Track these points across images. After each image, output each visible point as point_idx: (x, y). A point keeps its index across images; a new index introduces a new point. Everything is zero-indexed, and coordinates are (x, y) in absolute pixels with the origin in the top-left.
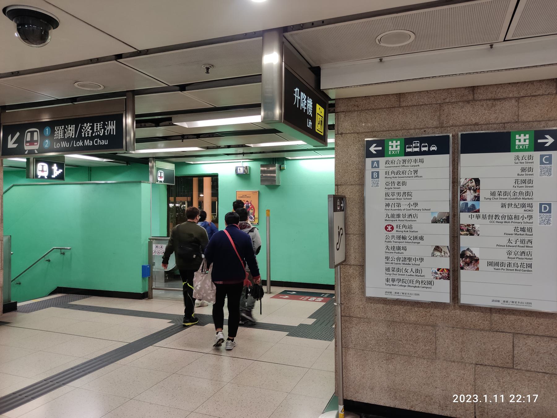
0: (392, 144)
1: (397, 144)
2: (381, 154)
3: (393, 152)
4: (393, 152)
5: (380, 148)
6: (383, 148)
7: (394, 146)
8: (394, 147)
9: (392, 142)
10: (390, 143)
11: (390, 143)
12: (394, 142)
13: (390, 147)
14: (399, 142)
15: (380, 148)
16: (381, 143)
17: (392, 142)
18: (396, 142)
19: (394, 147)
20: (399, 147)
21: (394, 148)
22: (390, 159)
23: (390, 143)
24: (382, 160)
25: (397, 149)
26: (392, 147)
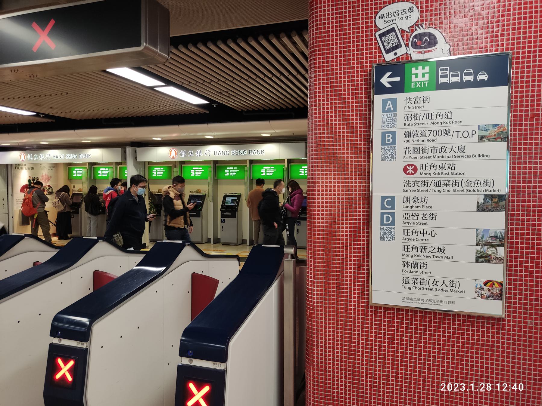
0: (416, 72)
1: (424, 71)
3: (418, 85)
4: (418, 85)
6: (402, 79)
8: (420, 75)
9: (417, 69)
13: (413, 77)
14: (427, 69)
17: (417, 69)
18: (424, 68)
19: (420, 75)
20: (427, 76)
21: (420, 78)
25: (424, 79)
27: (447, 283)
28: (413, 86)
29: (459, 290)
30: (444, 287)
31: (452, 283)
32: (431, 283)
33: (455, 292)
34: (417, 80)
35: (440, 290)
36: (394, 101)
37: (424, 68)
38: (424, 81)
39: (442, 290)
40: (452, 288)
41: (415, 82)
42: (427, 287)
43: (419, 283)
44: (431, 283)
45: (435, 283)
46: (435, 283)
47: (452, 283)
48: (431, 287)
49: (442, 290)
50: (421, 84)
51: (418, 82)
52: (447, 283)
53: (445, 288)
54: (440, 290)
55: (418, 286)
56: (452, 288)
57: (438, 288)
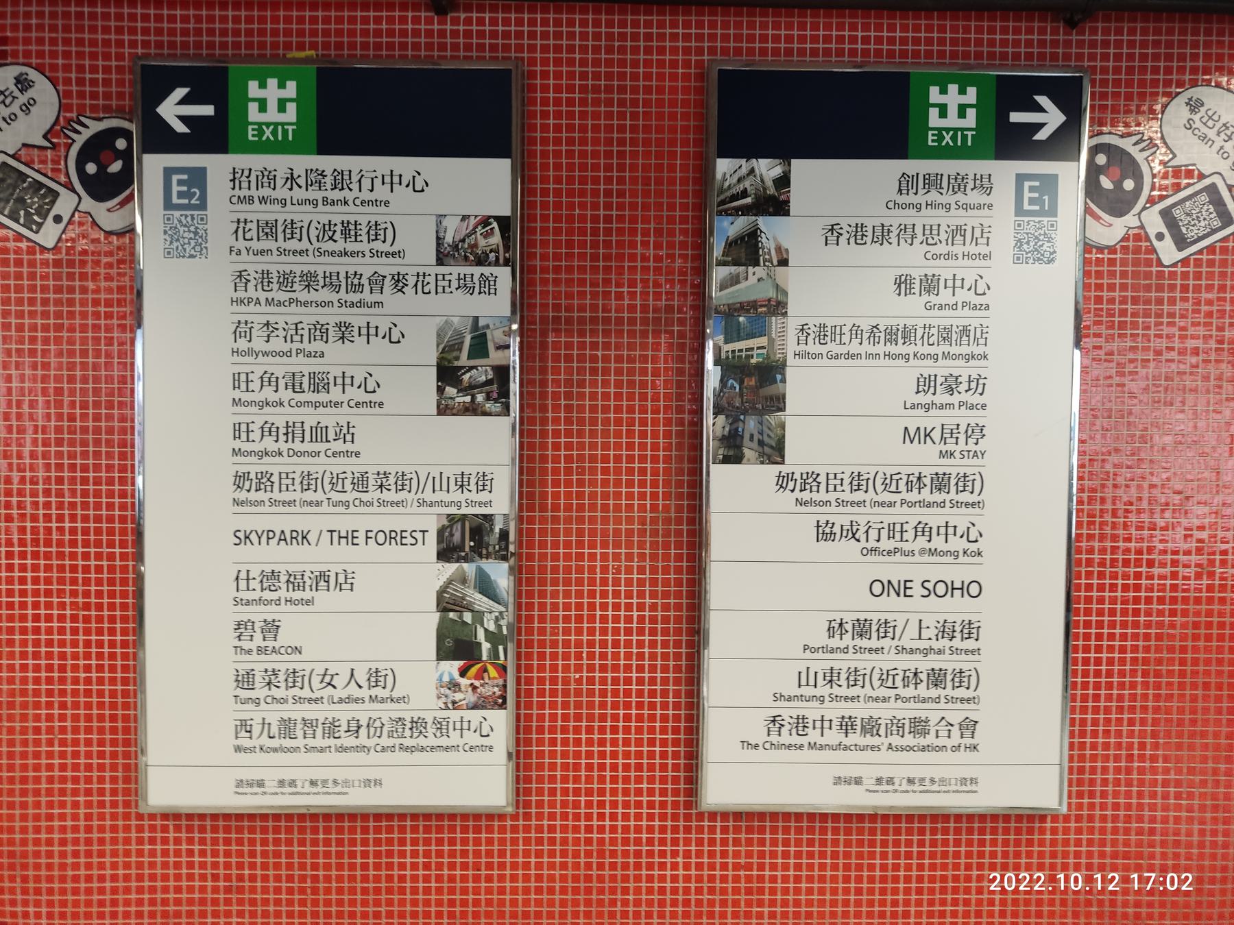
0: (260, 94)
2: (211, 136)
3: (268, 133)
4: (268, 133)
5: (208, 110)
7: (273, 101)
8: (272, 105)
9: (263, 85)
10: (253, 86)
11: (253, 86)
12: (272, 83)
13: (253, 108)
15: (208, 110)
16: (211, 84)
17: (263, 85)
18: (282, 85)
22: (257, 162)
23: (253, 89)
24: (217, 166)
25: (282, 118)
26: (263, 105)
27: (361, 677)
28: (251, 134)
29: (395, 694)
30: (353, 690)
31: (375, 678)
32: (316, 680)
33: (383, 700)
34: (262, 118)
35: (341, 701)
36: (198, 178)
37: (282, 85)
38: (283, 124)
39: (349, 699)
40: (374, 692)
41: (260, 124)
42: (306, 693)
43: (283, 685)
44: (316, 680)
45: (327, 679)
46: (327, 679)
47: (375, 678)
48: (318, 694)
49: (349, 699)
50: (274, 133)
51: (268, 125)
52: (361, 677)
53: (358, 693)
54: (341, 701)
55: (279, 693)
56: (374, 692)
57: (338, 694)
